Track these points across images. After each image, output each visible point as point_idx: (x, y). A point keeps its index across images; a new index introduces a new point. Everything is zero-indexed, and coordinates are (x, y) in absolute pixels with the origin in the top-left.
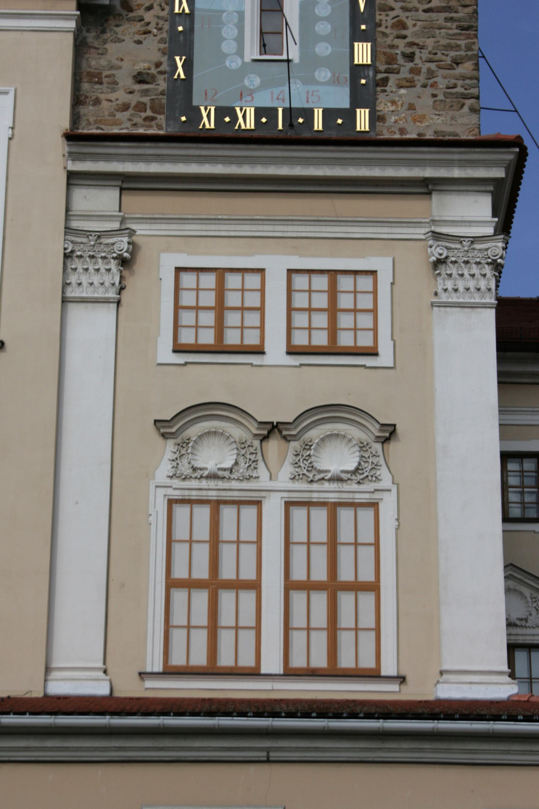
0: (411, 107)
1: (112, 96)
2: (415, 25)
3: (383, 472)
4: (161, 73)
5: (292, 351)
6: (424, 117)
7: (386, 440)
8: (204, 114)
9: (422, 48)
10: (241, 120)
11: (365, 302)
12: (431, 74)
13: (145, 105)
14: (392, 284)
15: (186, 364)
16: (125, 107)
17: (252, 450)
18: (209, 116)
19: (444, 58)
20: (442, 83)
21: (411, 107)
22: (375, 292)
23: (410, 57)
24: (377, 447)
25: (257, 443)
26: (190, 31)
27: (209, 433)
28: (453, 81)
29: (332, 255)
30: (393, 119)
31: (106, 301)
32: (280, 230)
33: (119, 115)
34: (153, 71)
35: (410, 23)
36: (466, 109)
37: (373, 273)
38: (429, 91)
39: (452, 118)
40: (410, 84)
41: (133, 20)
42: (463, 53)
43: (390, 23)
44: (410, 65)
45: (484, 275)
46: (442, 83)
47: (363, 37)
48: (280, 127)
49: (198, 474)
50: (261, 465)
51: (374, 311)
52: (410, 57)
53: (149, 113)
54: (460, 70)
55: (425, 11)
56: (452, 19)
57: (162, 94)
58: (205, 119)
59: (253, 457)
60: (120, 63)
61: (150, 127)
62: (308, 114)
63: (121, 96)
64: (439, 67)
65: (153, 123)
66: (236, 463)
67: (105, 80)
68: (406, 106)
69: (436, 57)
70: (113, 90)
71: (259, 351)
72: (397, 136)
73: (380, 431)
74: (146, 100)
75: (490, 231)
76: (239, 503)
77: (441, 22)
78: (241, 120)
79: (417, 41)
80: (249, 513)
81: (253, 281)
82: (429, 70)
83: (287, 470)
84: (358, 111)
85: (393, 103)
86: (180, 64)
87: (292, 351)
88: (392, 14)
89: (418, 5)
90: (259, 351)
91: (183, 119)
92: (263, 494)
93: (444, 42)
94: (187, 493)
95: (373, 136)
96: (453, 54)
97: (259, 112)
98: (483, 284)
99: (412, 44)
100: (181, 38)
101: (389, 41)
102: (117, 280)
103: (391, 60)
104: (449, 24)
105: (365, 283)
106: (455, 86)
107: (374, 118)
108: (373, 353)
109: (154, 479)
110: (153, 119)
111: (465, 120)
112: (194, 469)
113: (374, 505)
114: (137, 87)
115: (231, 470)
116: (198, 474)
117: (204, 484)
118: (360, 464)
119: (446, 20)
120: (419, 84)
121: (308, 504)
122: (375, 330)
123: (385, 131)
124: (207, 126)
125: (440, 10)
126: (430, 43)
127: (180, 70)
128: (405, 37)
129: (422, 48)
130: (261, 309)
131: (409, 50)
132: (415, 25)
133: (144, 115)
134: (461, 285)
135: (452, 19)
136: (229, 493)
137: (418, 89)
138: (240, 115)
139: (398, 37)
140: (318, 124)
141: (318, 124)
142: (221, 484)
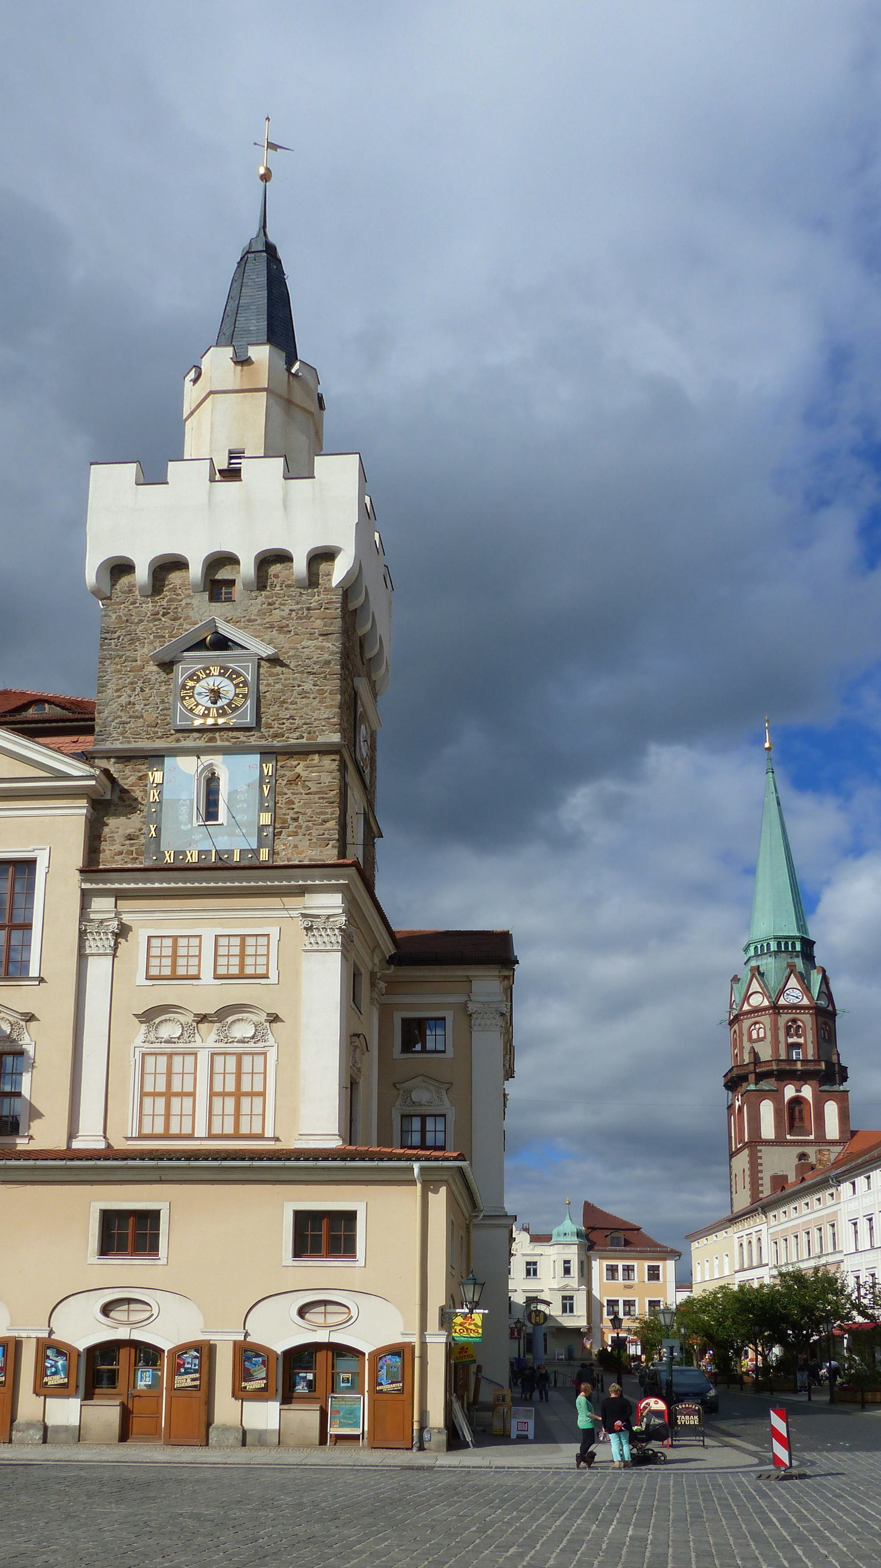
0: (296, 846)
1: (112, 848)
2: (299, 802)
3: (270, 1036)
4: (142, 834)
5: (216, 977)
6: (303, 851)
7: (271, 1022)
8: (167, 855)
9: (305, 814)
10: (189, 857)
11: (262, 950)
12: (308, 828)
13: (132, 851)
14: (279, 941)
15: (153, 985)
16: (121, 853)
17: (191, 1028)
18: (170, 856)
19: (317, 819)
20: (315, 833)
21: (296, 846)
22: (268, 945)
23: (296, 820)
24: (268, 1024)
25: (194, 1024)
26: (159, 812)
27: (166, 1020)
28: (322, 832)
29: (243, 927)
30: (284, 853)
31: (106, 955)
32: (211, 915)
33: (116, 858)
34: (138, 833)
35: (296, 801)
36: (329, 846)
37: (268, 935)
38: (308, 837)
39: (320, 852)
40: (295, 834)
41: (125, 806)
42: (329, 816)
43: (284, 801)
44: (296, 823)
45: (335, 935)
46: (315, 833)
47: (267, 810)
48: (213, 860)
49: (159, 1040)
50: (197, 1035)
51: (268, 955)
52: (296, 820)
53: (135, 855)
54: (328, 825)
55: (306, 794)
56: (323, 798)
57: (143, 845)
58: (168, 858)
59: (192, 1032)
60: (117, 830)
61: (135, 863)
62: (231, 852)
63: (117, 847)
64: (314, 824)
65: (137, 861)
66: (182, 1034)
67: (108, 839)
68: (292, 846)
69: (312, 819)
70: (113, 845)
71: (197, 977)
72: (286, 863)
73: (267, 1016)
74: (133, 849)
75: (341, 911)
76: (184, 1054)
77: (316, 800)
78: (189, 857)
79: (300, 811)
80: (190, 1059)
81: (195, 942)
82: (307, 826)
83: (213, 1036)
84: (261, 850)
85: (284, 844)
86: (153, 829)
87: (216, 977)
88: (287, 796)
89: (302, 791)
90: (197, 977)
91: (155, 858)
92: (198, 1049)
93: (318, 810)
94: (153, 1050)
95: (270, 863)
96: (322, 817)
97: (200, 853)
98: (333, 939)
99: (298, 812)
100: (155, 815)
101: (283, 811)
102: (112, 944)
103: (285, 821)
104: (321, 801)
105: (263, 941)
106: (324, 834)
107: (273, 853)
108: (265, 977)
109: (133, 1042)
110: (137, 859)
111: (329, 852)
112: (157, 1038)
113: (265, 1054)
114: (128, 842)
115: (179, 1038)
116: (159, 1040)
117: (163, 1045)
118: (255, 1033)
119: (319, 798)
120: (301, 834)
121: (225, 1054)
122: (267, 965)
123: (278, 860)
124: (169, 861)
125: (316, 793)
126: (309, 811)
127: (153, 832)
128: (293, 809)
129: (305, 814)
130: (199, 956)
131: (296, 816)
132: (299, 802)
133: (131, 857)
134: (319, 940)
135: (323, 798)
136: (177, 1050)
137: (300, 837)
138: (189, 855)
139: (289, 809)
140: (236, 858)
141: (236, 858)
142: (173, 1045)
